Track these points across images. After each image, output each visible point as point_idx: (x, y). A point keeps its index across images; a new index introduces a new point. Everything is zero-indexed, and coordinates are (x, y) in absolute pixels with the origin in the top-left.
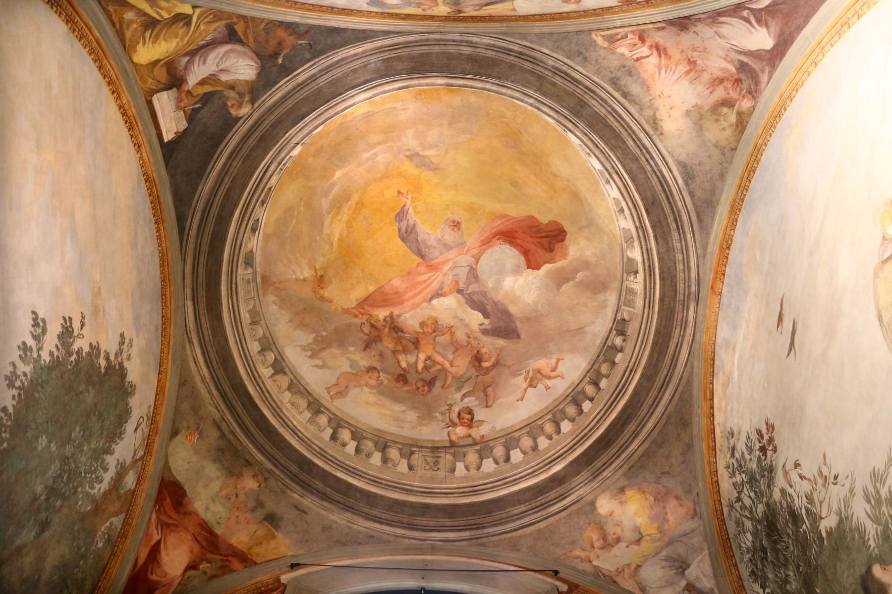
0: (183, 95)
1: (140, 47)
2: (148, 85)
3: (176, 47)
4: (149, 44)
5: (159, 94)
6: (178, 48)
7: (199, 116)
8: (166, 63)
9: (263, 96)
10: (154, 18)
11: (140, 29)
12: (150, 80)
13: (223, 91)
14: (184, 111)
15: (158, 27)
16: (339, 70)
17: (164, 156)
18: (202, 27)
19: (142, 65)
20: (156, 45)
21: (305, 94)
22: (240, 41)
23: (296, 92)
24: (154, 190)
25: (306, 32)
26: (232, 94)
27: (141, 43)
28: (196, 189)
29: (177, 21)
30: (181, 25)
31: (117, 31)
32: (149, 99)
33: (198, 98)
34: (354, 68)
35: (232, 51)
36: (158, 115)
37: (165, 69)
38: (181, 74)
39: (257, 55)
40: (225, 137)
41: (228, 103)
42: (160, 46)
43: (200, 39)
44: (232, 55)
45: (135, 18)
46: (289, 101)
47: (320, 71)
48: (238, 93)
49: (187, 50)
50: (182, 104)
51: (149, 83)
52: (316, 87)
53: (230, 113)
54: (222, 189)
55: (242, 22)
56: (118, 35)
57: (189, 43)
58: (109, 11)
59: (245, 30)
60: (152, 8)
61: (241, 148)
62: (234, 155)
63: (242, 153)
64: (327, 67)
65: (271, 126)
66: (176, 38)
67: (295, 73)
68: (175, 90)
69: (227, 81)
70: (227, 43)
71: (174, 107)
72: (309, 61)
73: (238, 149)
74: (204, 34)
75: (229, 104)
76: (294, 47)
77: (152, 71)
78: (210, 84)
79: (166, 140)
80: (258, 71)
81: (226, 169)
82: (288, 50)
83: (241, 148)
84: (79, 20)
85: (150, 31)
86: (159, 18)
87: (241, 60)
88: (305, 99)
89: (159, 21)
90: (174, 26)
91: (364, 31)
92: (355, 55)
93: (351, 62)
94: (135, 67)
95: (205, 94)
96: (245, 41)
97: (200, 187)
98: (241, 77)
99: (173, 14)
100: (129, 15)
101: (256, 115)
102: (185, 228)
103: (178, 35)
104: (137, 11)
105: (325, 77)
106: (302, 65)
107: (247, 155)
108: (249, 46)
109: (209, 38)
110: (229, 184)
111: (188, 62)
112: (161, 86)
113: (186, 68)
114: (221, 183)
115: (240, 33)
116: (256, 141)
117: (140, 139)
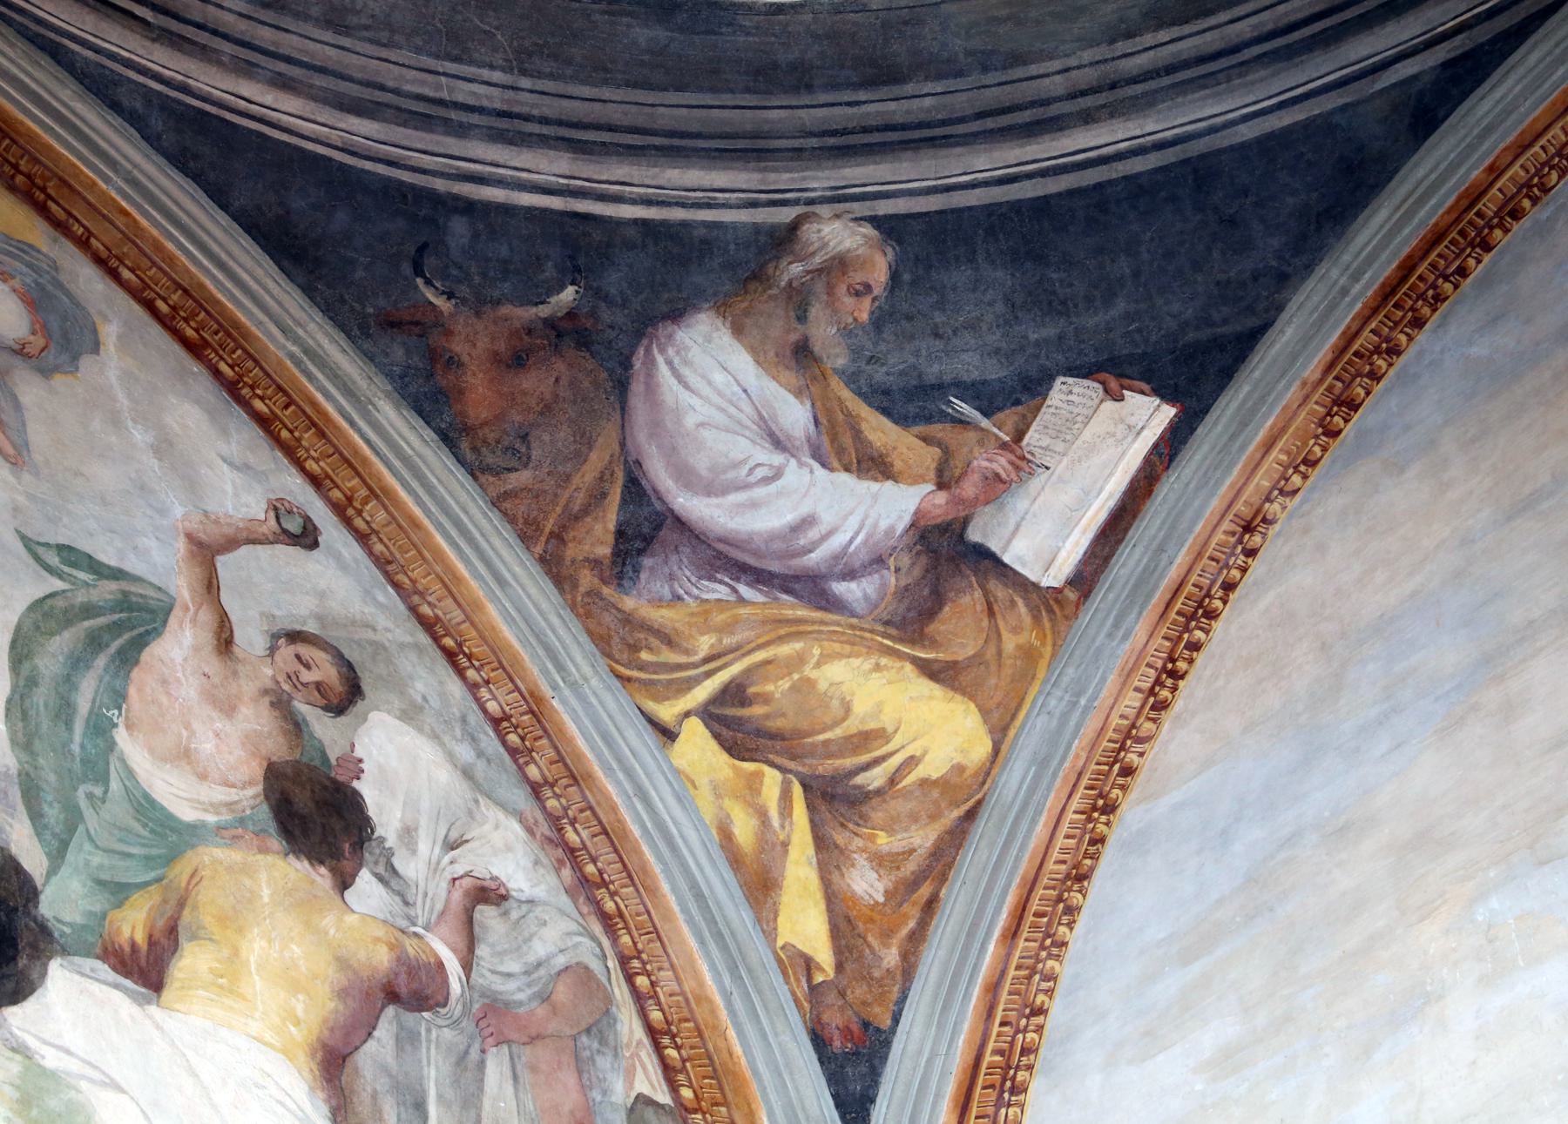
0: (969, 488)
1: (934, 766)
2: (1029, 636)
3: (840, 656)
4: (901, 746)
5: (1031, 574)
6: (837, 647)
7: (994, 371)
8: (912, 642)
9: (734, 226)
10: (811, 807)
11: (878, 816)
12: (1010, 643)
13: (840, 373)
14: (1019, 436)
15: (827, 766)
16: (389, 75)
17: (1227, 375)
18: (705, 644)
19: (985, 713)
20: (887, 721)
21: (586, 91)
22: (636, 488)
23: (611, 129)
24: (1366, 339)
25: (392, 324)
26: (823, 332)
27: (920, 772)
28: (1266, 144)
29: (760, 733)
30: (757, 710)
31: (943, 879)
32: (1072, 595)
33: (936, 430)
34: (328, 36)
35: (687, 478)
36: (1103, 516)
37: (936, 628)
38: (905, 560)
39: (622, 387)
40: (989, 209)
41: (864, 317)
42: (879, 708)
43: (744, 611)
44: (701, 463)
45: (861, 860)
46: (667, 117)
47: (462, 131)
48: (802, 318)
49: (818, 615)
50: (1001, 464)
51: (1022, 639)
52: (525, 83)
53: (895, 276)
54: (1187, 48)
55: (571, 552)
56: (950, 865)
57: (794, 627)
58: (905, 956)
59: (586, 511)
60: (785, 845)
61: (980, 115)
62: (1026, 116)
63: (992, 97)
64: (424, 122)
65: (809, 88)
66: (810, 683)
67: (556, 203)
68: (974, 535)
69: (798, 393)
70: (681, 523)
71: (1035, 484)
72: (469, 207)
73: (990, 123)
74: (720, 618)
75: (864, 311)
76: (480, 304)
77: (977, 659)
78: (857, 434)
79: (1169, 412)
80: (671, 327)
81: (1101, 99)
82: (506, 310)
83: (980, 115)
84: (991, 1046)
85: (859, 780)
86: (797, 790)
87: (690, 421)
88: (600, 71)
89: (806, 787)
90: (778, 724)
91: (181, 161)
92: (283, 84)
93: (322, 70)
94: (1005, 730)
95: (903, 420)
96: (620, 476)
97: (1247, 132)
98: (742, 361)
99: (749, 766)
100: (866, 884)
101: (820, 179)
102: (1445, 65)
103: (794, 688)
104: (835, 877)
105: (464, 92)
106: (507, 210)
107: (985, 69)
108: (623, 444)
109: (721, 592)
110: (1148, 39)
111: (850, 575)
112: (1000, 591)
113: (879, 561)
114: (1170, 69)
115: (609, 517)
116: (909, 88)
117: (1219, 536)
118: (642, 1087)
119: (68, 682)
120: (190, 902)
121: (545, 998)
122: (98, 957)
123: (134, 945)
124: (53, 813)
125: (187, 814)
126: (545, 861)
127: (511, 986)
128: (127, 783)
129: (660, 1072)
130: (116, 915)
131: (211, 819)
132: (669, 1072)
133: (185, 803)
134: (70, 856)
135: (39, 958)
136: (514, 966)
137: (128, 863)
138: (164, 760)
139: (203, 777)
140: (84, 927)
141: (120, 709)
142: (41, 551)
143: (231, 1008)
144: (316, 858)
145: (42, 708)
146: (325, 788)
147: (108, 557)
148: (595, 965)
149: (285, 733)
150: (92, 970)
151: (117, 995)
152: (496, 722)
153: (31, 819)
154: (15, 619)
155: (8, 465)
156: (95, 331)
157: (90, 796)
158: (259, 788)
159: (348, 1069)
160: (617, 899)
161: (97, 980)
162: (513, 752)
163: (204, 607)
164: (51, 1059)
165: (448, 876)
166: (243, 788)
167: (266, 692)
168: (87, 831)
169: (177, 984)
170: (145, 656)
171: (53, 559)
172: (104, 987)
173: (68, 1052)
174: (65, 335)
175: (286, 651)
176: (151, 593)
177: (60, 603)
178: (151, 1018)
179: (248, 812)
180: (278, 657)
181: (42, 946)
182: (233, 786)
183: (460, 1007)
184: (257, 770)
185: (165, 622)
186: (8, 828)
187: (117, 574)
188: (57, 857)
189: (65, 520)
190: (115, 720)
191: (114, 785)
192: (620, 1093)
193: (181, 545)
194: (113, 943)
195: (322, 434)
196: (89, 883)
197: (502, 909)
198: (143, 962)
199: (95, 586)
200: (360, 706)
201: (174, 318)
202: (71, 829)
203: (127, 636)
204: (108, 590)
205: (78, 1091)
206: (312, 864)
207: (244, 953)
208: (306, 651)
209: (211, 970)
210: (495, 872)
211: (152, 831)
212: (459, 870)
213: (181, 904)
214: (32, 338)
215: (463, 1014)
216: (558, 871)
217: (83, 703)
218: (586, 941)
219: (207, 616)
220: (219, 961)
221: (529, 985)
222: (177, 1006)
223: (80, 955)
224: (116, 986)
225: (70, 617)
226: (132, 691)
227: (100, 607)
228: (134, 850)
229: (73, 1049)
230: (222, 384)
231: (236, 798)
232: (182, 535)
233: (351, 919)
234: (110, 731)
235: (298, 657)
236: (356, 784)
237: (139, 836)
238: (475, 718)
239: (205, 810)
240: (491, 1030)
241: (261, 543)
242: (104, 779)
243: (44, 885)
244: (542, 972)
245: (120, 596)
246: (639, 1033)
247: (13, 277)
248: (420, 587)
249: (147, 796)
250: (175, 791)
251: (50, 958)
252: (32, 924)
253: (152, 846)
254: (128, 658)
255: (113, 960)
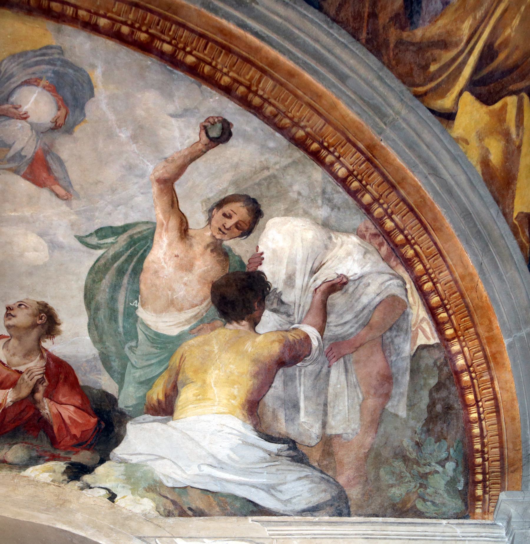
118: (422, 341)
119: (113, 299)
120: (181, 371)
121: (367, 324)
122: (145, 413)
123: (159, 402)
124: (116, 364)
125: (174, 332)
126: (371, 248)
127: (347, 327)
128: (146, 333)
129: (433, 329)
130: (150, 392)
131: (187, 328)
132: (439, 327)
133: (173, 327)
134: (127, 379)
135: (122, 425)
136: (348, 317)
137: (153, 368)
138: (161, 312)
139: (180, 310)
140: (137, 405)
141: (137, 299)
142: (88, 240)
143: (205, 406)
144: (238, 319)
145: (103, 320)
146: (243, 280)
147: (119, 223)
148: (398, 292)
149: (219, 262)
150: (144, 419)
151: (155, 424)
152: (343, 182)
153: (108, 371)
154: (84, 283)
155: (64, 202)
156: (90, 81)
157: (131, 348)
158: (209, 299)
159: (261, 404)
160: (416, 247)
161: (146, 422)
162: (353, 194)
163: (171, 218)
164: (134, 460)
165: (312, 289)
166: (201, 304)
167: (208, 246)
168: (132, 364)
169: (179, 408)
170: (146, 264)
171: (94, 241)
172: (150, 424)
173: (140, 454)
174: (75, 99)
175: (218, 215)
176: (145, 227)
177: (103, 261)
178: (171, 426)
179: (204, 315)
180: (213, 222)
181: (122, 420)
182: (197, 305)
183: (317, 352)
184: (207, 290)
185: (152, 240)
186: (100, 380)
187: (125, 228)
188: (121, 382)
189: (97, 214)
190: (136, 306)
191: (141, 336)
192: (407, 349)
193: (155, 189)
194: (150, 405)
195: (229, 51)
196: (137, 385)
197: (344, 290)
198: (164, 406)
199: (117, 242)
200: (261, 221)
201: (133, 33)
202: (124, 367)
203: (135, 260)
204: (123, 239)
205: (147, 466)
206: (238, 323)
207: (208, 382)
208: (227, 209)
209: (194, 395)
210: (339, 272)
211: (161, 348)
212: (319, 282)
213: (177, 374)
214: (59, 113)
215: (319, 354)
216: (378, 251)
217: (121, 307)
218: (395, 282)
219: (174, 223)
220: (197, 390)
221: (356, 323)
222: (181, 417)
223: (138, 416)
224: (154, 421)
225: (106, 268)
226: (142, 287)
227: (121, 252)
228: (153, 361)
229: (142, 452)
230: (166, 61)
231: (199, 310)
232: (155, 182)
233: (259, 339)
234: (135, 312)
235: (224, 215)
236: (260, 268)
237: (155, 354)
238: (332, 186)
239: (184, 325)
240: (334, 355)
241: (198, 157)
242: (136, 337)
243: (119, 396)
244: (366, 311)
245: (129, 240)
246: (423, 313)
247: (41, 79)
248: (296, 120)
249: (157, 334)
250: (168, 324)
251: (126, 423)
252: (117, 413)
253: (161, 355)
254: (137, 271)
255: (151, 412)
